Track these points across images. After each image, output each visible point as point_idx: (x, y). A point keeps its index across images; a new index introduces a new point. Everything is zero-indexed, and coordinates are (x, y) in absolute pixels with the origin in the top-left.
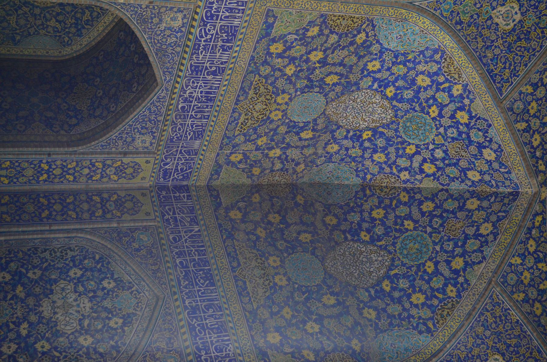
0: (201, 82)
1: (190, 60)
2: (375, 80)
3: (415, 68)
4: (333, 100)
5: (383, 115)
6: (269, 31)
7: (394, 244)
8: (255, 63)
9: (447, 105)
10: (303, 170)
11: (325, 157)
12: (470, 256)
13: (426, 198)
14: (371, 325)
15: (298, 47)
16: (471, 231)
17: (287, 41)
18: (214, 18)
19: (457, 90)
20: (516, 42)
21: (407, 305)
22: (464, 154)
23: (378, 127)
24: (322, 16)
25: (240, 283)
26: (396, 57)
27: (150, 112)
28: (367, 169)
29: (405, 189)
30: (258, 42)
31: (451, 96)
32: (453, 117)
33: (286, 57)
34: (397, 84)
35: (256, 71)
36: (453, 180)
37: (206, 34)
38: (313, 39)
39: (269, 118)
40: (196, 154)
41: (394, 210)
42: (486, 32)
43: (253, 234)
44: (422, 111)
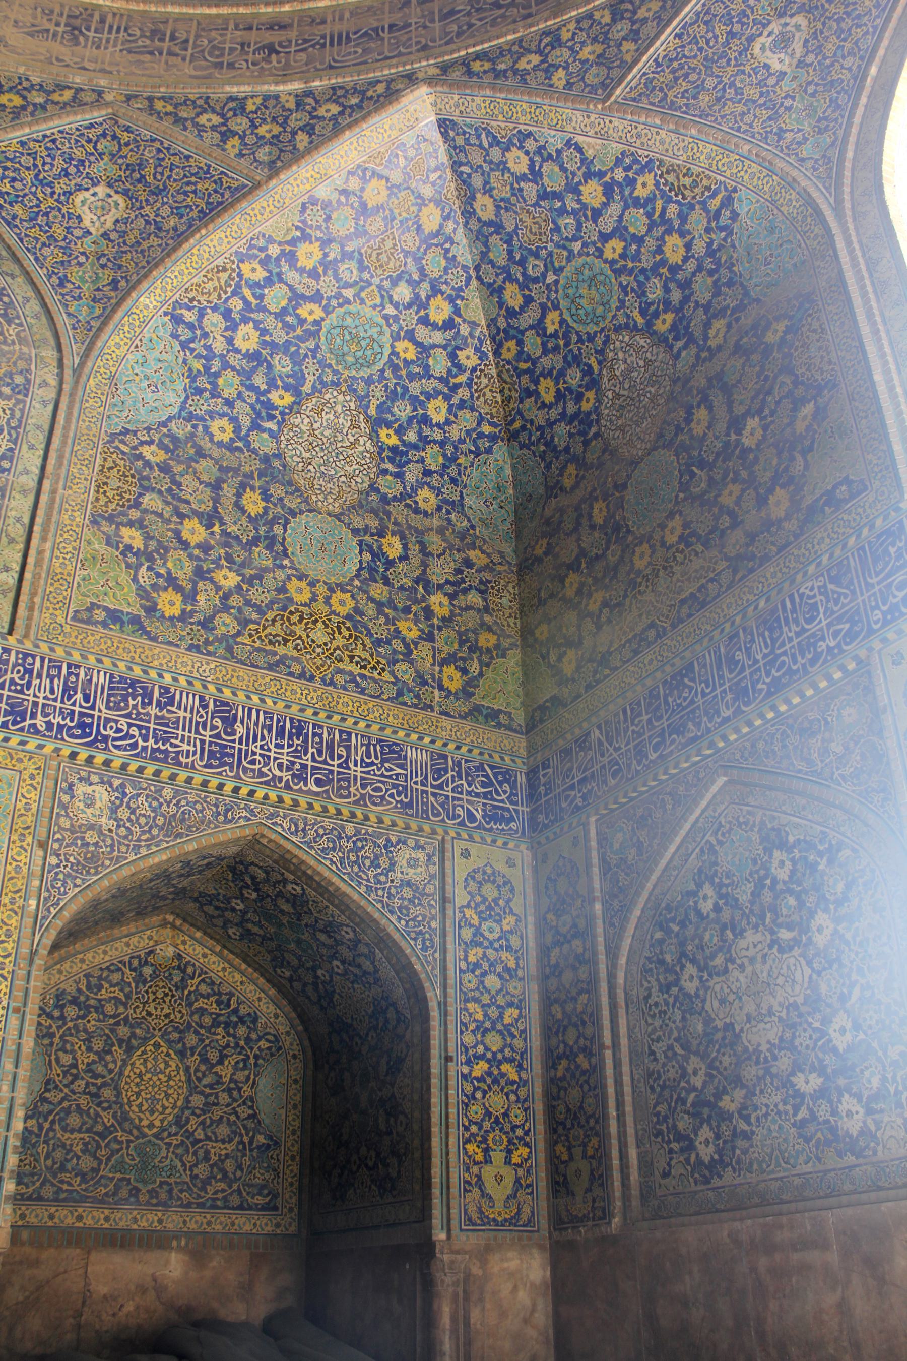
0: (252, 747)
1: (193, 767)
2: (256, 427)
3: (222, 356)
4: (306, 501)
5: (339, 408)
6: (125, 619)
7: (591, 338)
8: (207, 642)
9: (291, 287)
10: (483, 552)
11: (448, 512)
12: (574, 174)
13: (501, 304)
14: (737, 320)
15: (170, 565)
16: (530, 190)
17: (154, 586)
18: (88, 721)
19: (254, 272)
21: (691, 265)
23: (368, 418)
24: (94, 522)
25: (685, 610)
26: (199, 391)
27: (334, 849)
28: (468, 433)
29: (497, 353)
30: (154, 639)
32: (314, 274)
33: (195, 584)
34: (263, 387)
35: (229, 644)
36: (452, 260)
37: (128, 736)
38: (152, 538)
39: (349, 617)
40: (445, 757)
41: (534, 363)
42: (131, 239)
43: (599, 617)
44: (315, 334)
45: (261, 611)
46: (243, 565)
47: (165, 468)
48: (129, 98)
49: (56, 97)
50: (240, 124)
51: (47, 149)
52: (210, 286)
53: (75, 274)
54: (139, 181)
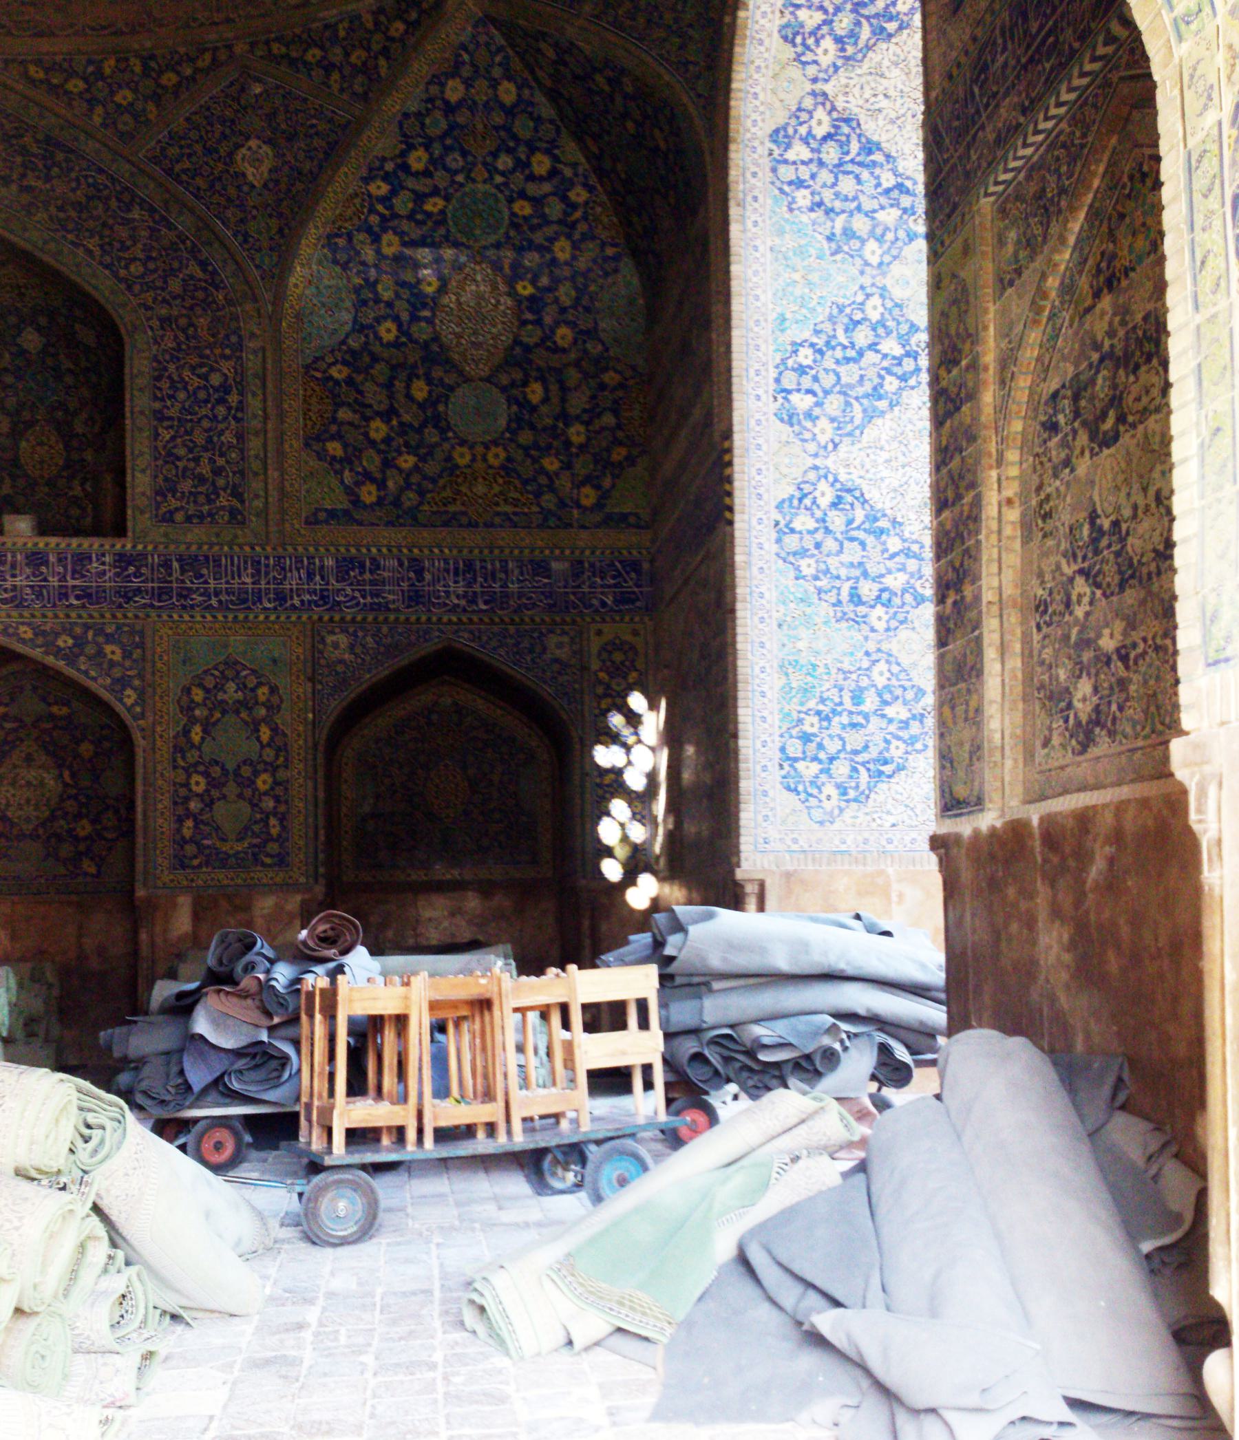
2: (414, 318)
8: (398, 517)
19: (380, 188)
22: (480, 127)
23: (504, 276)
24: (307, 445)
26: (365, 303)
28: (594, 261)
30: (360, 523)
31: (393, 193)
32: (426, 173)
33: (383, 472)
36: (538, 120)
39: (503, 467)
40: (581, 562)
42: (283, 186)
45: (434, 481)
46: (418, 447)
47: (350, 381)
52: (349, 212)
53: (252, 227)
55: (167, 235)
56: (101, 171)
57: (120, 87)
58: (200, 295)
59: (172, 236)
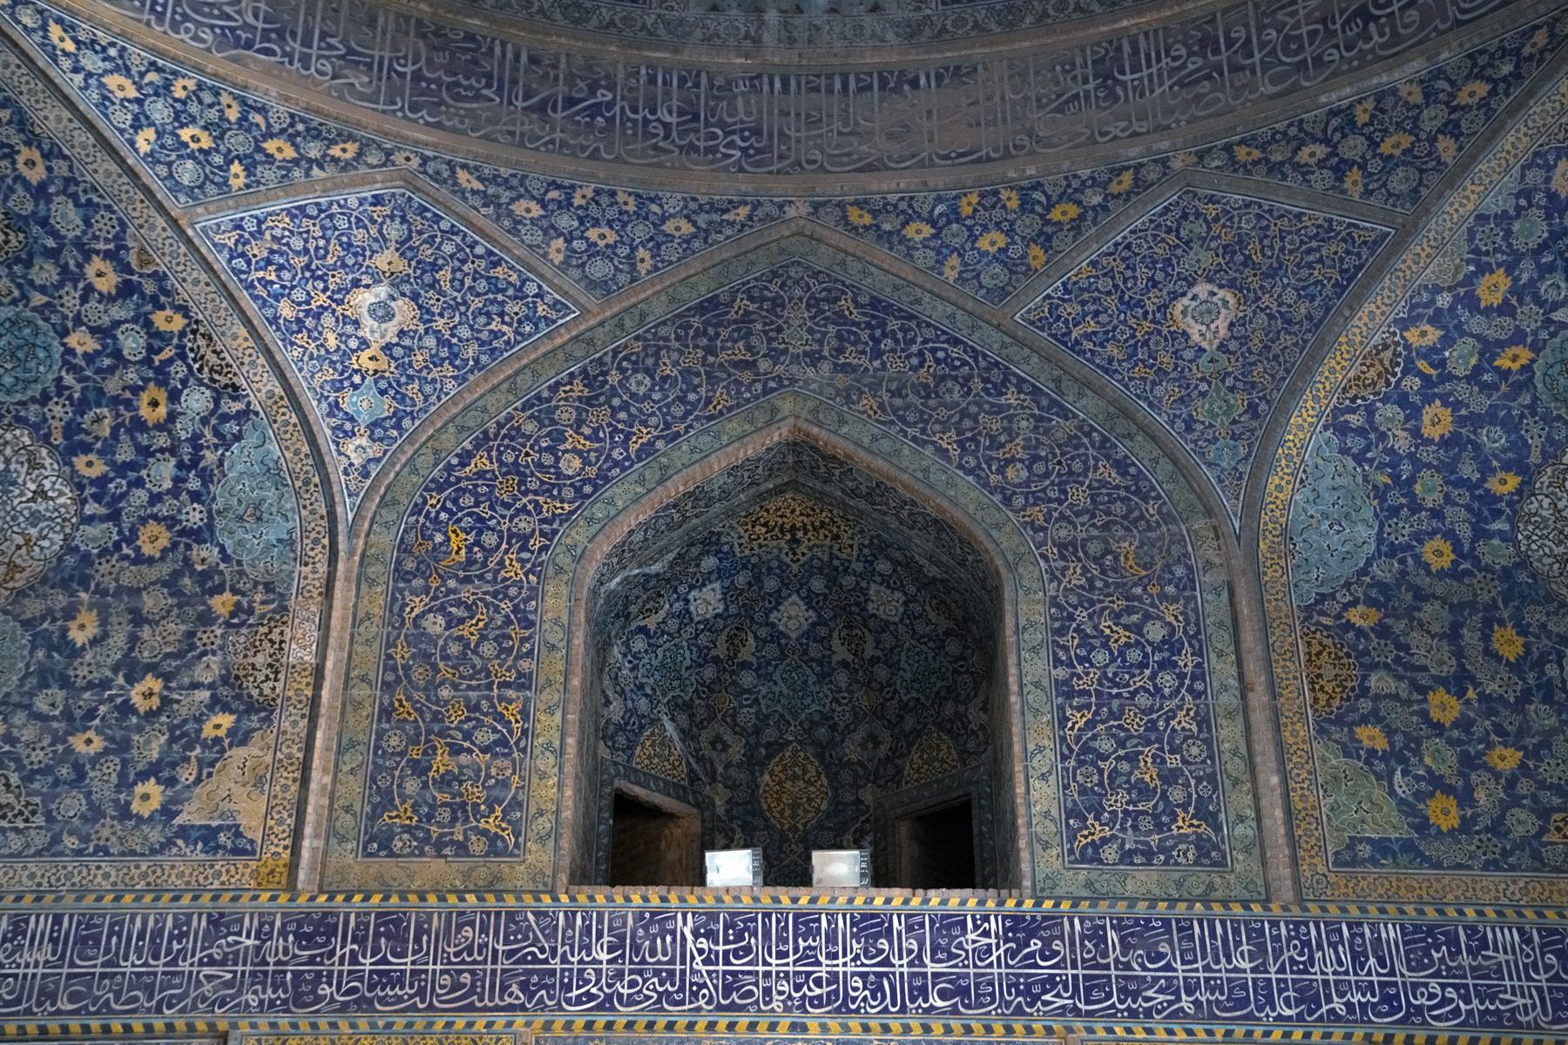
1: (1538, 1027)
3: (1411, 456)
6: (1396, 847)
9: (1477, 337)
15: (1428, 760)
17: (1416, 794)
18: (1392, 991)
19: (1425, 335)
20: (1255, 266)
24: (1322, 731)
26: (1395, 511)
30: (1438, 865)
31: (1447, 341)
32: (1505, 309)
33: (1466, 777)
35: (1533, 848)
37: (1445, 1001)
42: (1256, 344)
44: (1528, 384)
46: (1522, 732)
47: (1383, 631)
48: (1201, 156)
49: (1114, 188)
50: (1354, 147)
51: (1124, 260)
52: (1372, 373)
54: (1245, 264)
55: (1062, 428)
56: (956, 342)
57: (985, 228)
58: (1119, 509)
59: (1070, 426)
